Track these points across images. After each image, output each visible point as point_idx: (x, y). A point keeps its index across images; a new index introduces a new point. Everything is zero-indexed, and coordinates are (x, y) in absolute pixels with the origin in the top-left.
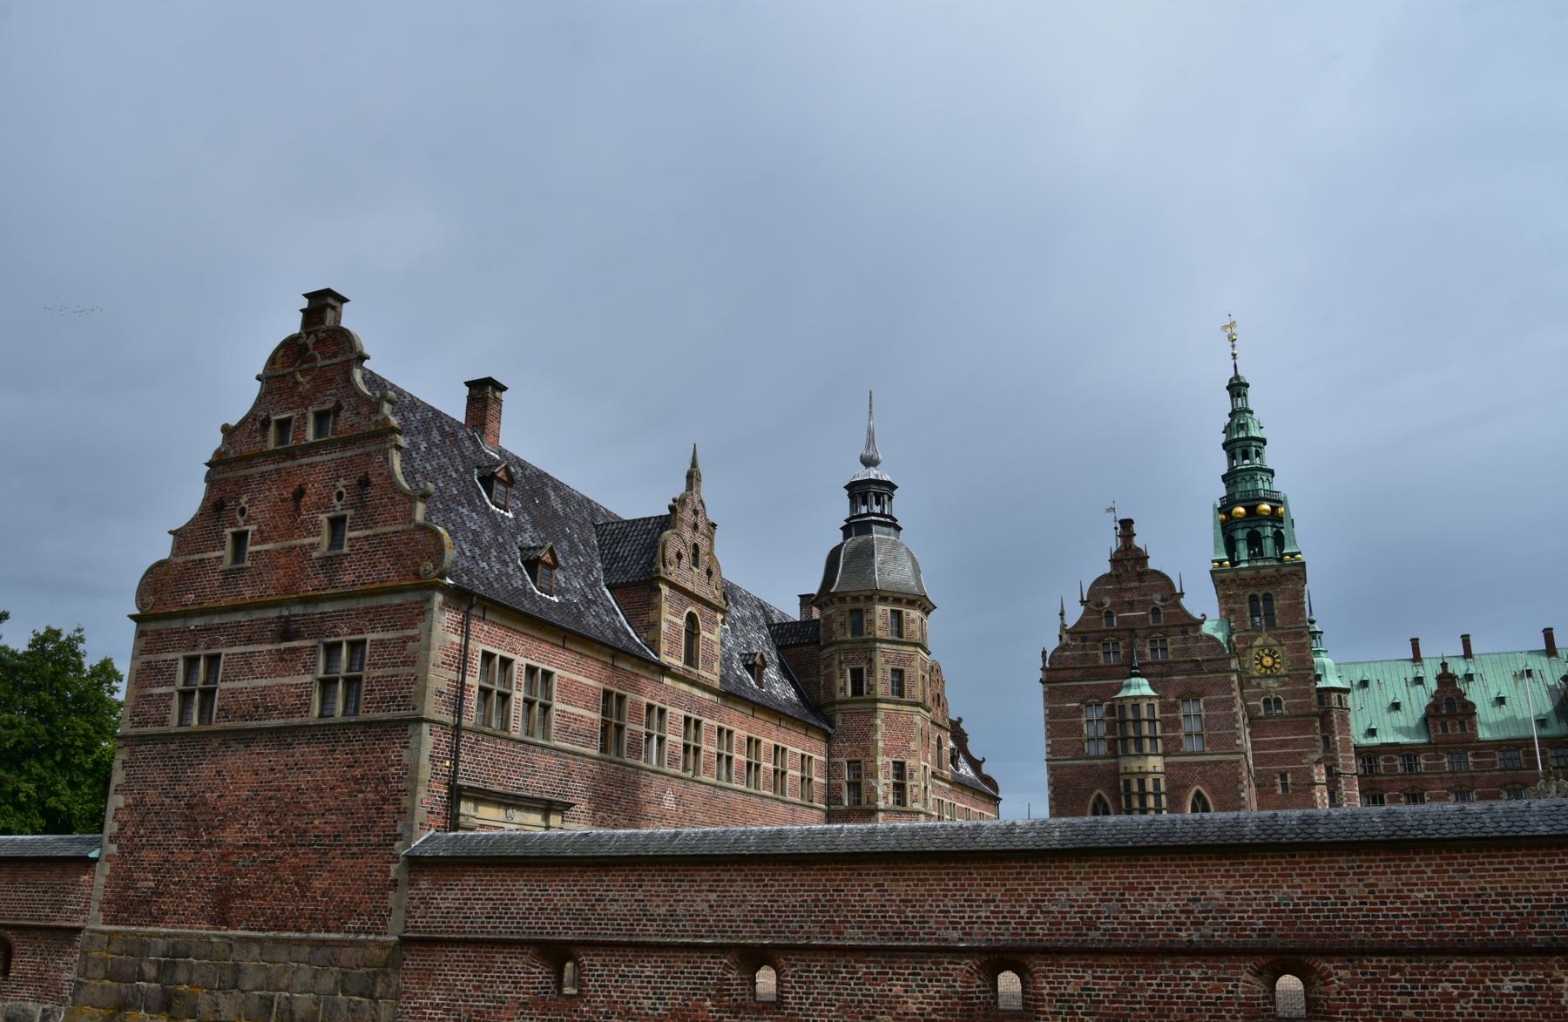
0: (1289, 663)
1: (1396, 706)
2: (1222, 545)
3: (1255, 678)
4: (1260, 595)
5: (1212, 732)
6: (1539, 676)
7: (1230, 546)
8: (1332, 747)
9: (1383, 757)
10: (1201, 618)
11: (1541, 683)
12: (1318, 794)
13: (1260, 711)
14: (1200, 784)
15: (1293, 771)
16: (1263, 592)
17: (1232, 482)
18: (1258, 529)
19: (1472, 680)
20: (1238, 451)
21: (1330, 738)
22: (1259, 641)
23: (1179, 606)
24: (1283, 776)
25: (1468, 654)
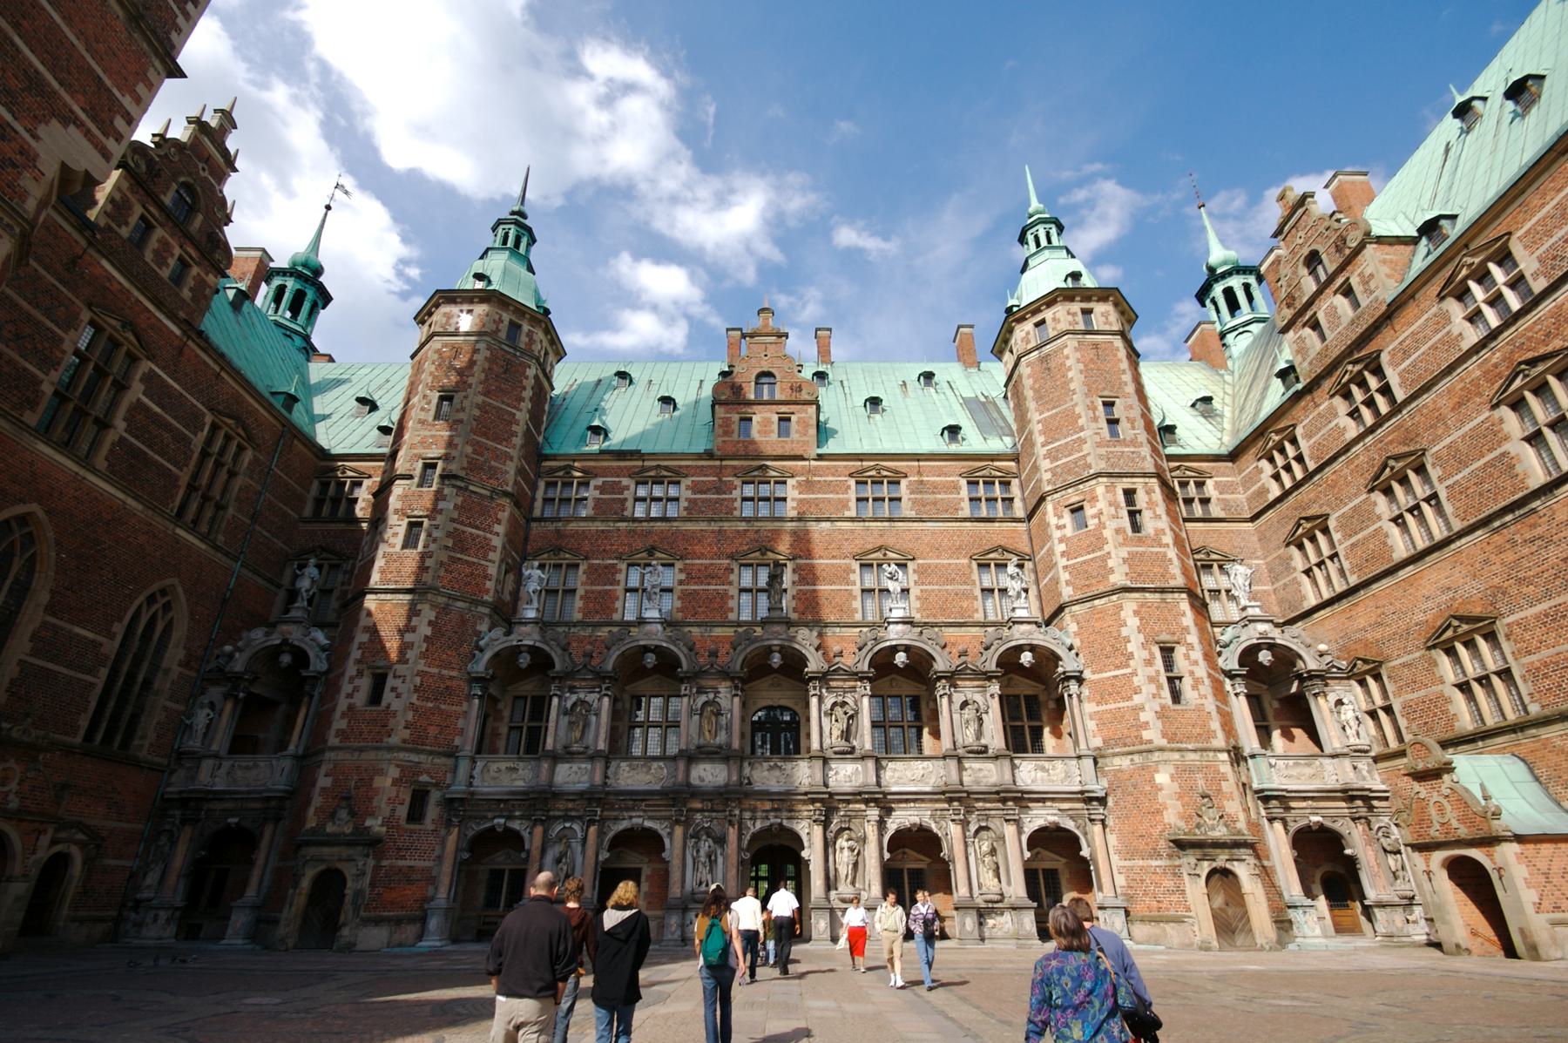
9: (599, 481)
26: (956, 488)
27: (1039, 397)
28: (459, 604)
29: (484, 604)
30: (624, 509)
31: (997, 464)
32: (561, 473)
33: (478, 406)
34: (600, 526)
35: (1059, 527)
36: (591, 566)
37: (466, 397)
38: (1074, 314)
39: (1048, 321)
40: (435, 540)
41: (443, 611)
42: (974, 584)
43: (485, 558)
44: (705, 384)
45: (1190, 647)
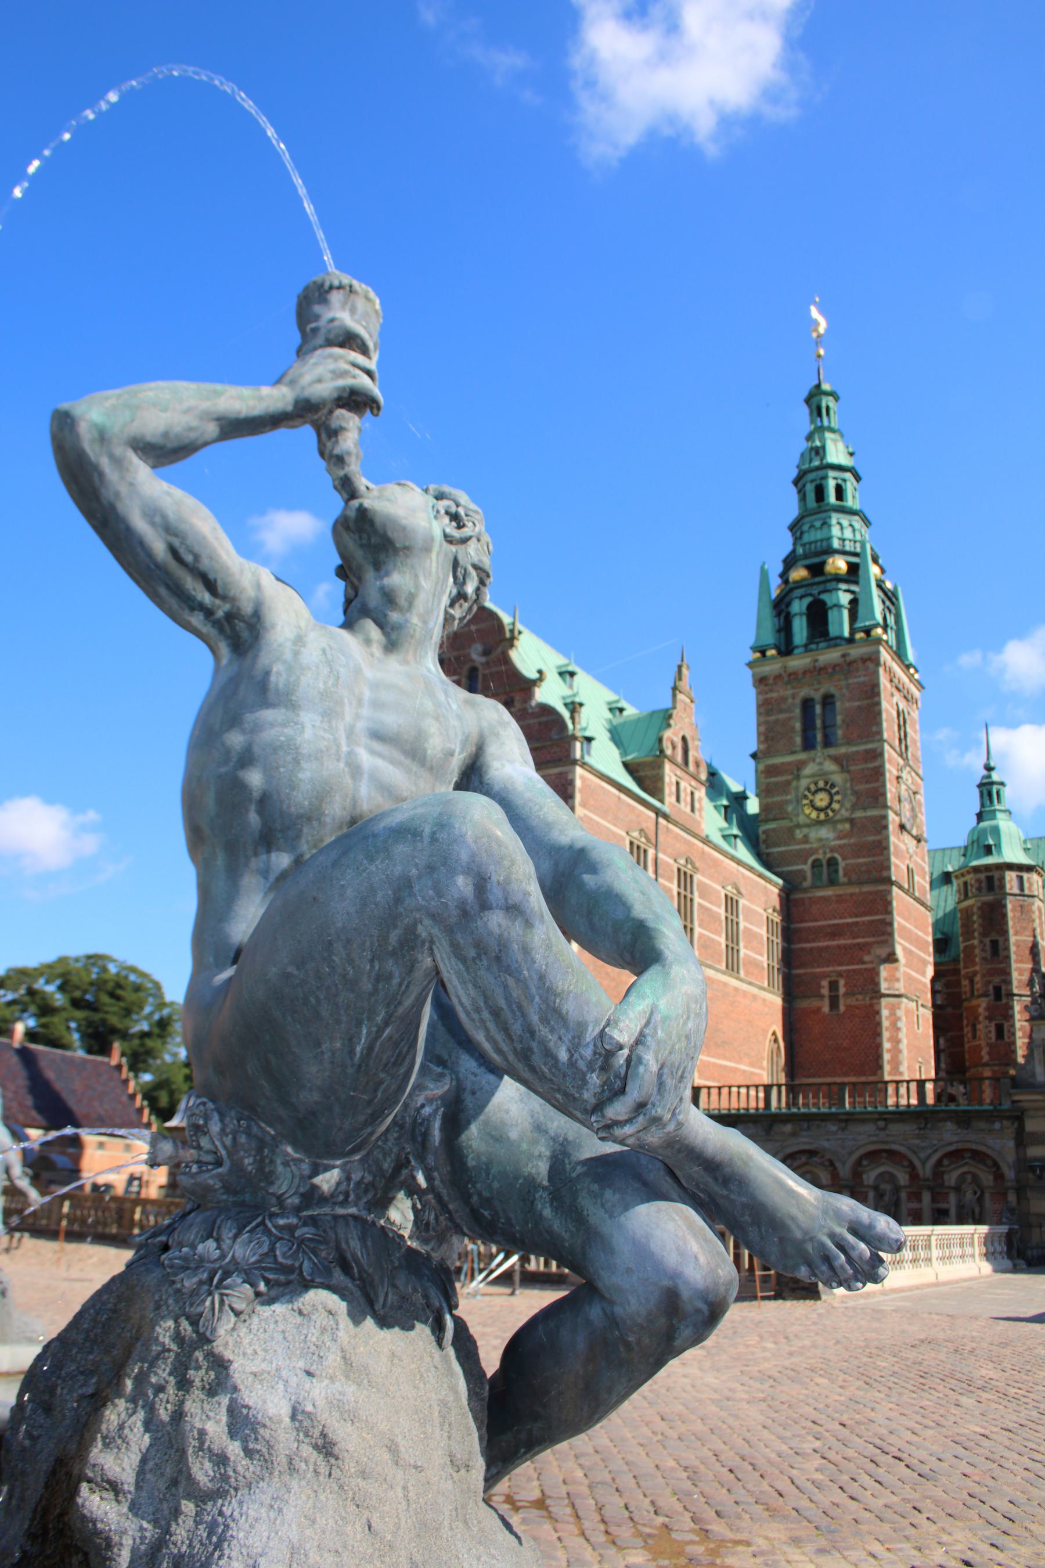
0: (853, 799)
2: (770, 624)
3: (798, 826)
4: (817, 696)
7: (785, 629)
8: (1002, 954)
10: (533, 675)
12: (885, 1012)
13: (805, 879)
15: (848, 975)
16: (822, 691)
17: (798, 534)
18: (824, 597)
20: (810, 489)
21: (1001, 940)
22: (809, 770)
23: (507, 661)
24: (833, 986)
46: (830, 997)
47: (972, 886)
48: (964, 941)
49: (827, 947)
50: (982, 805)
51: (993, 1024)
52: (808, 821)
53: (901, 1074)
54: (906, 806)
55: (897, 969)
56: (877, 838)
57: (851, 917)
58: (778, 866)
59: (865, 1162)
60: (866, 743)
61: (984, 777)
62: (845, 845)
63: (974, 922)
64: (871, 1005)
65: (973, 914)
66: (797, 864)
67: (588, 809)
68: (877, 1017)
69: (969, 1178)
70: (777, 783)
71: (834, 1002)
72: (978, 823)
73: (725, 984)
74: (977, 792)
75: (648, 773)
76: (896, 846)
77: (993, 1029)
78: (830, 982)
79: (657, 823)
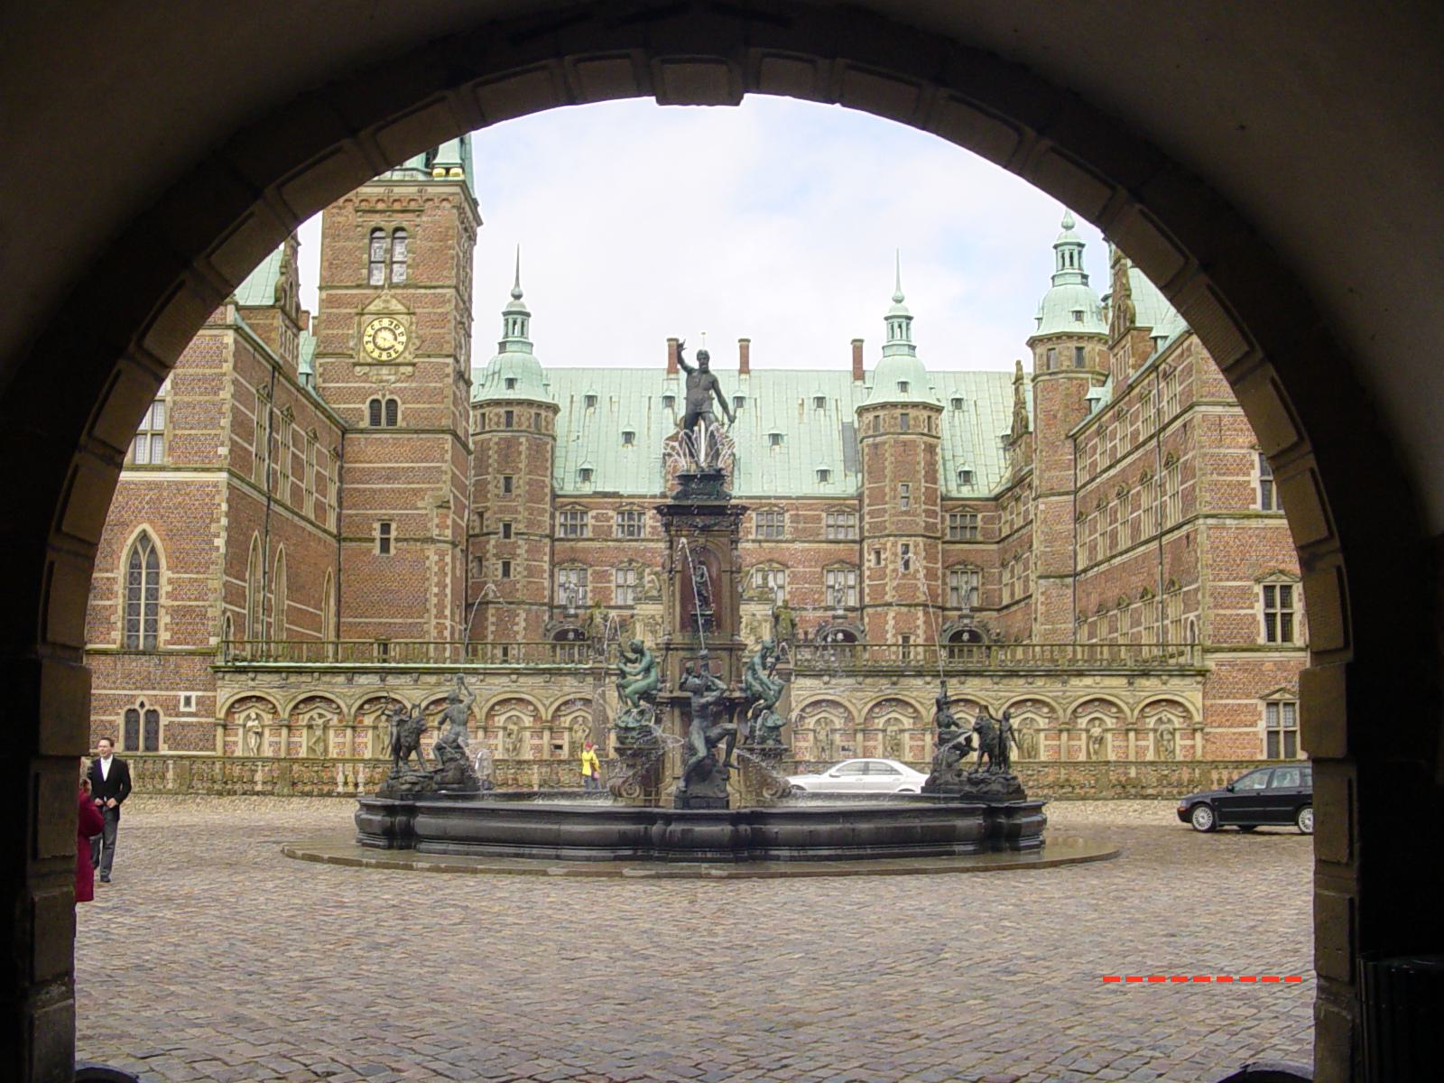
1: (629, 436)
5: (177, 432)
6: (834, 407)
8: (515, 492)
9: (593, 513)
11: (834, 418)
14: (151, 522)
16: (394, 224)
19: (742, 406)
24: (386, 528)
25: (744, 368)
26: (819, 519)
27: (869, 473)
28: (535, 607)
29: (544, 604)
30: (611, 533)
31: (848, 502)
32: (569, 507)
33: (528, 483)
34: (597, 544)
35: (869, 561)
36: (594, 572)
37: (520, 478)
38: (896, 418)
39: (881, 417)
40: (519, 573)
41: (528, 612)
42: (823, 583)
43: (542, 578)
44: (652, 400)
45: (918, 636)
46: (382, 539)
47: (490, 420)
48: (475, 476)
49: (382, 489)
50: (506, 335)
51: (500, 562)
52: (369, 360)
53: (446, 617)
54: (463, 351)
55: (447, 516)
56: (441, 385)
57: (407, 462)
58: (334, 403)
59: (497, 708)
60: (435, 287)
61: (511, 305)
62: (405, 388)
63: (489, 457)
64: (422, 550)
65: (490, 449)
66: (354, 402)
67: (238, 373)
68: (427, 563)
69: (580, 719)
70: (337, 315)
71: (385, 545)
72: (500, 353)
73: (304, 529)
74: (502, 319)
75: (261, 322)
76: (454, 394)
77: (500, 566)
78: (382, 525)
79: (273, 377)
